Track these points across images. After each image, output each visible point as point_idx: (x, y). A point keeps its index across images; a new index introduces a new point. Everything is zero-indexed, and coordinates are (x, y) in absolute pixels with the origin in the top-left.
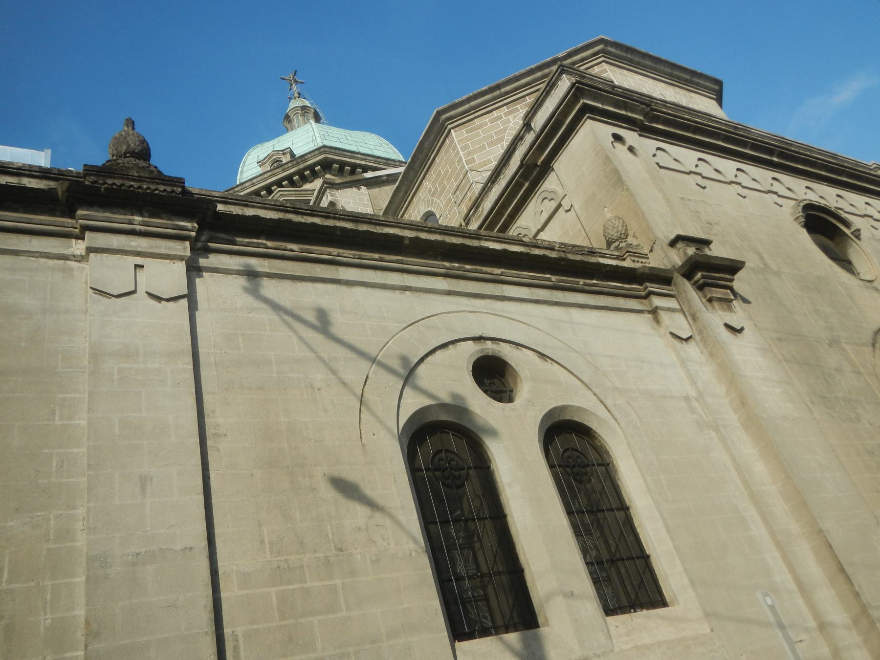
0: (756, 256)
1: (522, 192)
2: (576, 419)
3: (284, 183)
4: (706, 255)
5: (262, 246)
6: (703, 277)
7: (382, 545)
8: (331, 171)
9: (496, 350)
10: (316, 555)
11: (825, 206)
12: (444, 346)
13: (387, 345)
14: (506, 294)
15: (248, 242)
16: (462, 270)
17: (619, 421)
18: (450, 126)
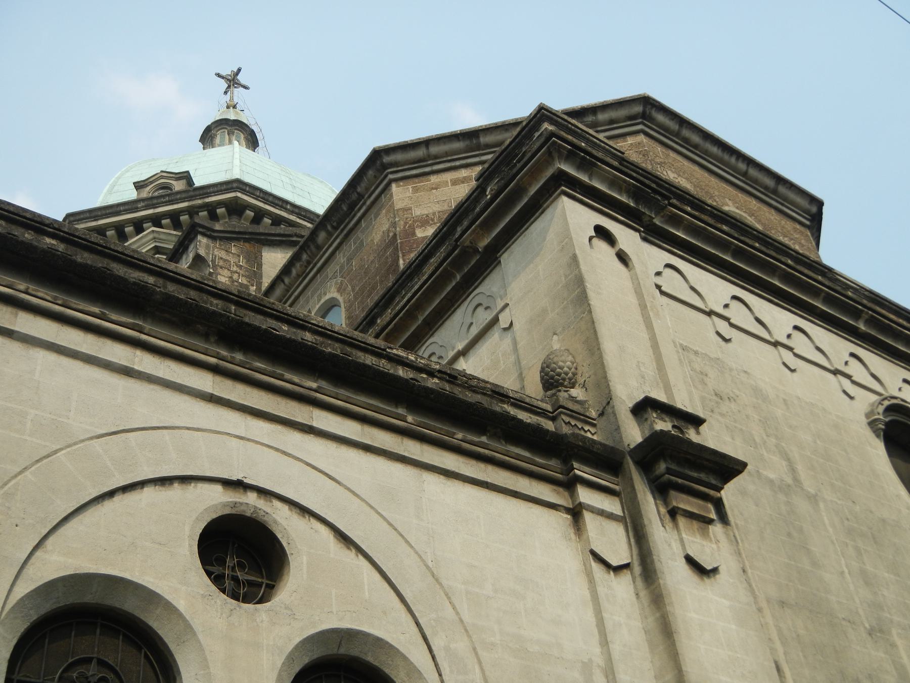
0: (784, 463)
1: (449, 288)
2: (370, 659)
3: (164, 222)
4: (690, 443)
6: (669, 471)
8: (240, 220)
12: (164, 481)
13: (54, 456)
14: (315, 424)
16: (247, 366)
18: (391, 176)
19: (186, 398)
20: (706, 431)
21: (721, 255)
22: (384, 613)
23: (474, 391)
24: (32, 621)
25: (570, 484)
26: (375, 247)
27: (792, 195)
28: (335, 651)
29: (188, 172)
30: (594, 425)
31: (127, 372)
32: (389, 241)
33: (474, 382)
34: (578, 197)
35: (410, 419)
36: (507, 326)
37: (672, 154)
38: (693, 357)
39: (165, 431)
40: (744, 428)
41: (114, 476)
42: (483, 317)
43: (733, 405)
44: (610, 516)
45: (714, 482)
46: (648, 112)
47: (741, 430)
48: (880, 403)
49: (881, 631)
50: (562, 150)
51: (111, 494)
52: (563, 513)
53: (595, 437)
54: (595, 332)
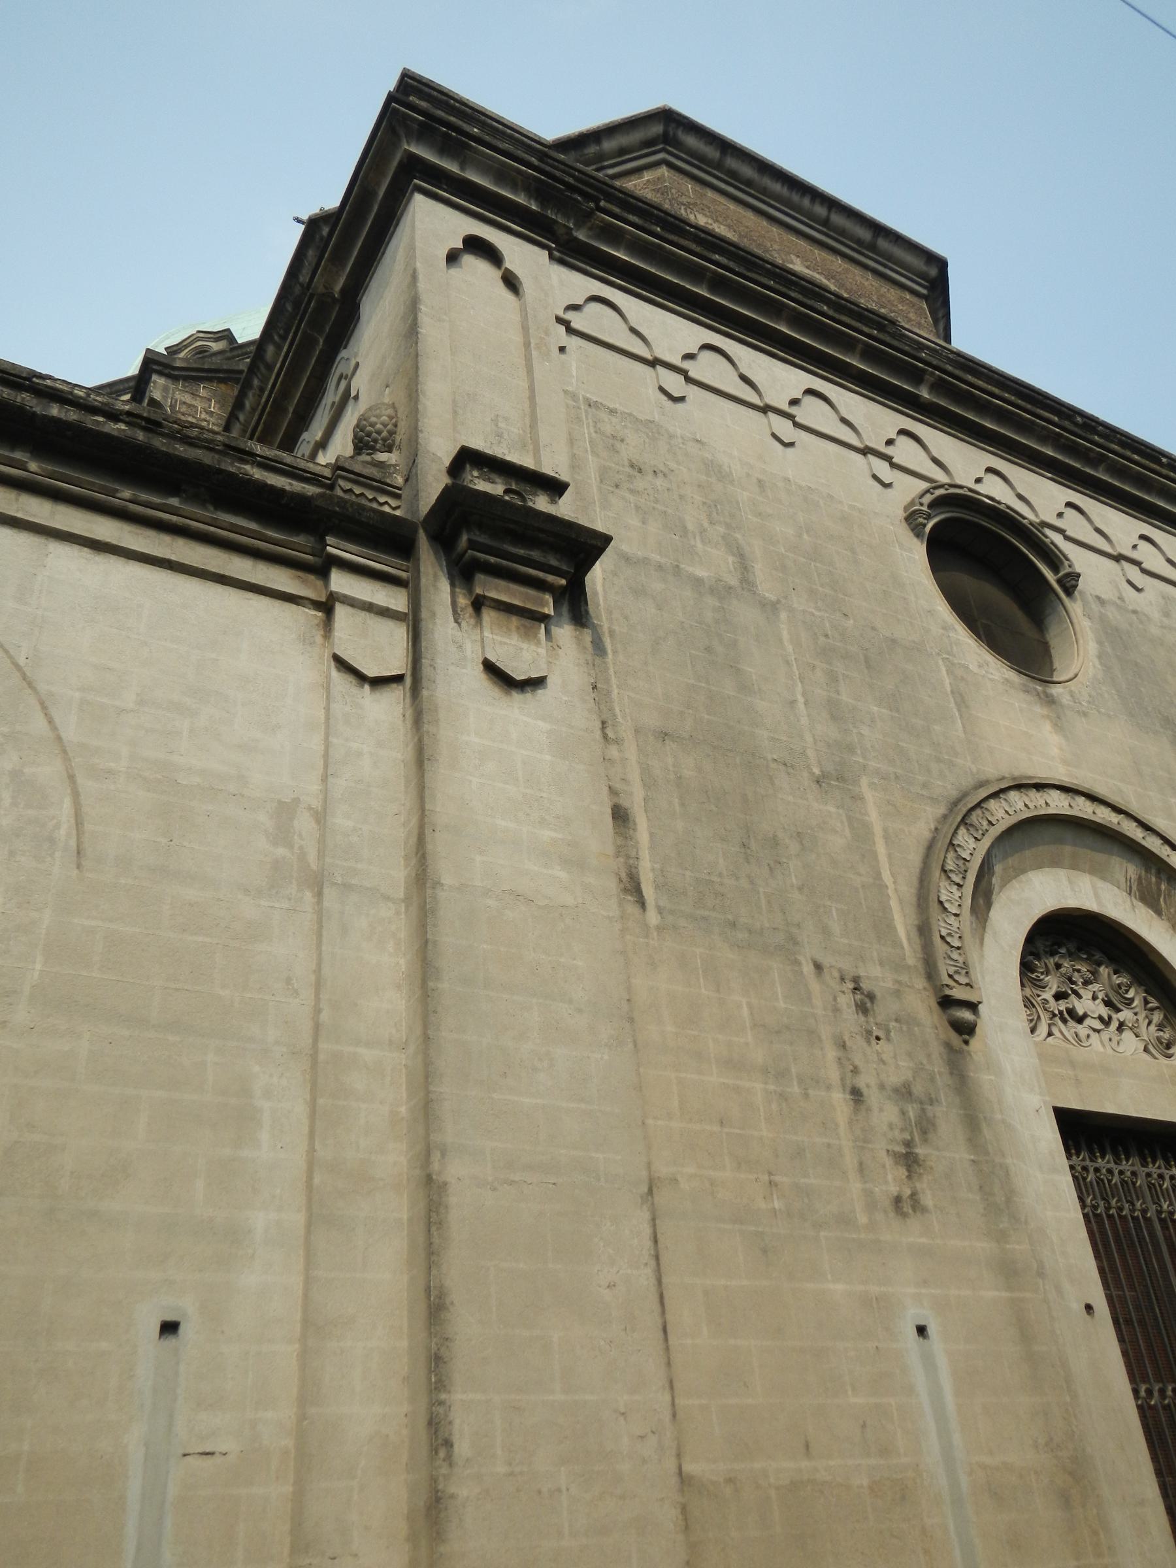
6: (472, 545)
20: (595, 511)
23: (192, 445)
27: (898, 252)
30: (397, 497)
33: (195, 432)
34: (442, 195)
35: (33, 466)
37: (710, 194)
38: (603, 415)
40: (670, 511)
43: (659, 482)
44: (384, 613)
46: (671, 133)
48: (927, 491)
49: (841, 778)
50: (408, 122)
52: (310, 609)
53: (398, 513)
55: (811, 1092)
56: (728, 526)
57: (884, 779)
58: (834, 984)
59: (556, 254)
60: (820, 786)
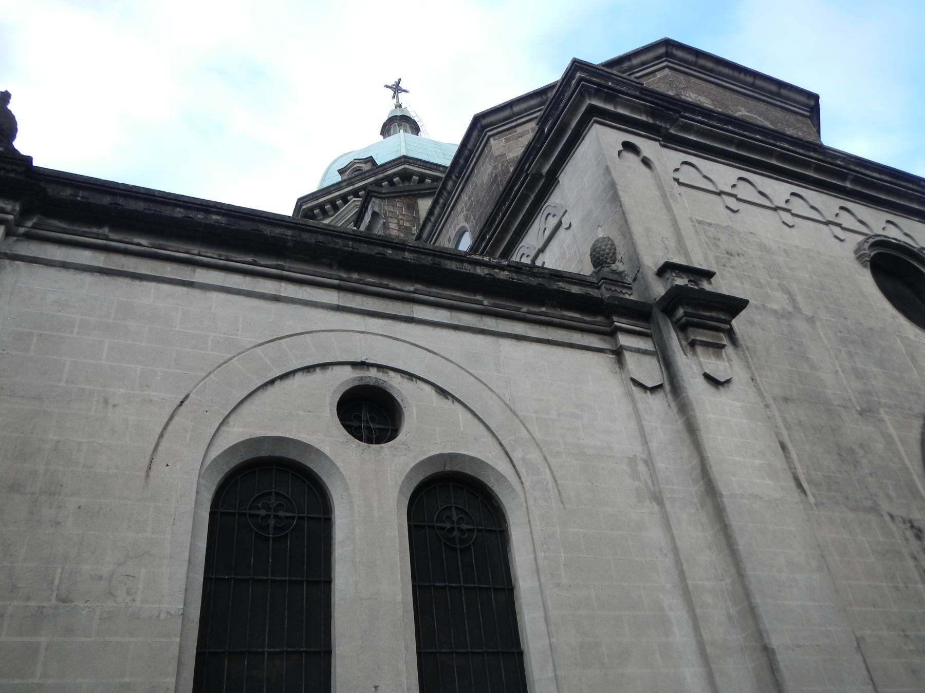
0: (785, 296)
1: (527, 206)
3: (360, 193)
4: (702, 291)
5: (101, 237)
6: (686, 314)
7: (124, 600)
9: (380, 379)
10: (28, 604)
11: (905, 245)
14: (415, 316)
15: (84, 232)
16: (361, 282)
17: (524, 479)
19: (321, 310)
20: (719, 281)
21: (726, 148)
22: (476, 440)
24: (225, 473)
25: (612, 333)
26: (485, 186)
27: (792, 95)
28: (442, 469)
29: (371, 157)
30: (630, 288)
31: (276, 299)
32: (493, 180)
36: (568, 226)
37: (693, 80)
38: (707, 228)
39: (307, 335)
40: (751, 275)
41: (272, 370)
42: (552, 222)
43: (742, 260)
44: (645, 352)
45: (723, 317)
47: (749, 276)
48: (866, 241)
50: (590, 90)
51: (272, 382)
53: (632, 298)
54: (626, 221)
55: (909, 585)
56: (779, 278)
57: (890, 408)
58: (901, 525)
59: (662, 142)
60: (863, 417)
